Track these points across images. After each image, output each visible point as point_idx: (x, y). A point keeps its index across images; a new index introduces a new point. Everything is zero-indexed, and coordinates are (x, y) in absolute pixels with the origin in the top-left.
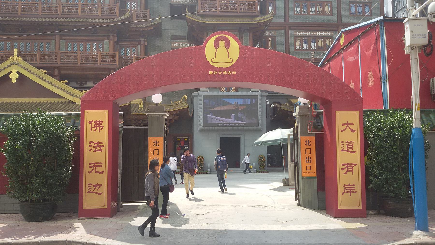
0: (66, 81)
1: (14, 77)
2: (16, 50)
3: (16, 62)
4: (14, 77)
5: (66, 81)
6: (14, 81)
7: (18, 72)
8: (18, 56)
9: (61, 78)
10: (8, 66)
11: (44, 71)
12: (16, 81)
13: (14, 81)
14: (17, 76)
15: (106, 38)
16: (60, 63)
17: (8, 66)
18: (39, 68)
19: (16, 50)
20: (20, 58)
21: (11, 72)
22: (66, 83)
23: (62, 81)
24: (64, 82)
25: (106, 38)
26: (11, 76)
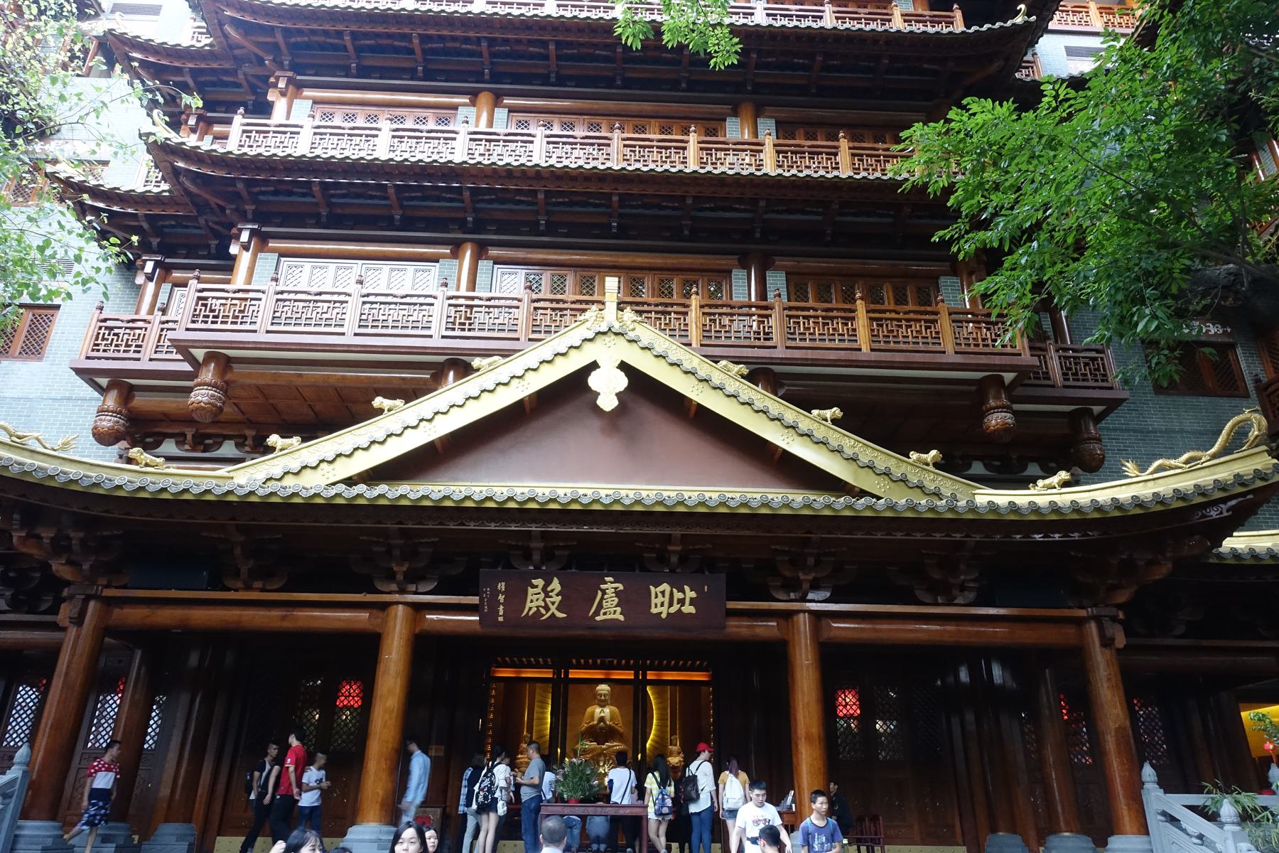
0: (836, 412)
1: (608, 387)
4: (608, 387)
6: (608, 402)
7: (623, 366)
11: (737, 368)
12: (615, 403)
13: (608, 402)
14: (622, 382)
18: (715, 359)
20: (629, 314)
21: (594, 366)
22: (834, 421)
23: (815, 412)
26: (594, 381)
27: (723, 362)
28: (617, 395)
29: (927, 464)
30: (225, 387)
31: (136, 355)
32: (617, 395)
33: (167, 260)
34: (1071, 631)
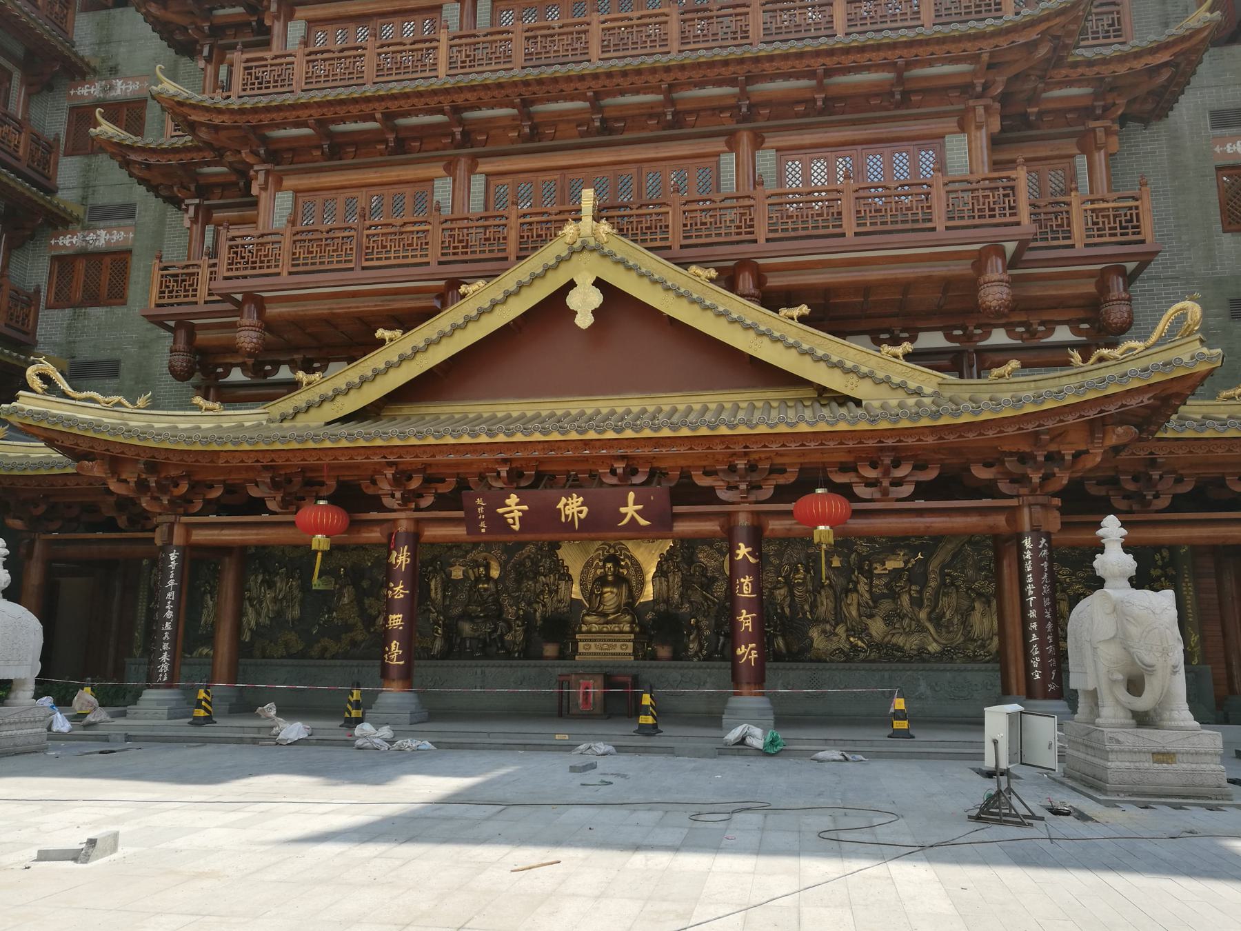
0: (804, 309)
1: (584, 304)
2: (588, 198)
3: (592, 243)
4: (584, 304)
5: (804, 309)
6: (584, 320)
7: (599, 283)
8: (597, 219)
9: (773, 300)
10: (560, 260)
13: (584, 320)
14: (596, 298)
15: (952, 123)
16: (768, 240)
17: (560, 260)
19: (588, 198)
20: (605, 227)
21: (571, 285)
22: (802, 319)
23: (783, 311)
24: (796, 312)
25: (952, 123)
26: (573, 300)
27: (693, 268)
28: (593, 312)
29: (896, 357)
30: (268, 326)
31: (194, 299)
32: (593, 312)
33: (206, 202)
34: (1001, 521)
